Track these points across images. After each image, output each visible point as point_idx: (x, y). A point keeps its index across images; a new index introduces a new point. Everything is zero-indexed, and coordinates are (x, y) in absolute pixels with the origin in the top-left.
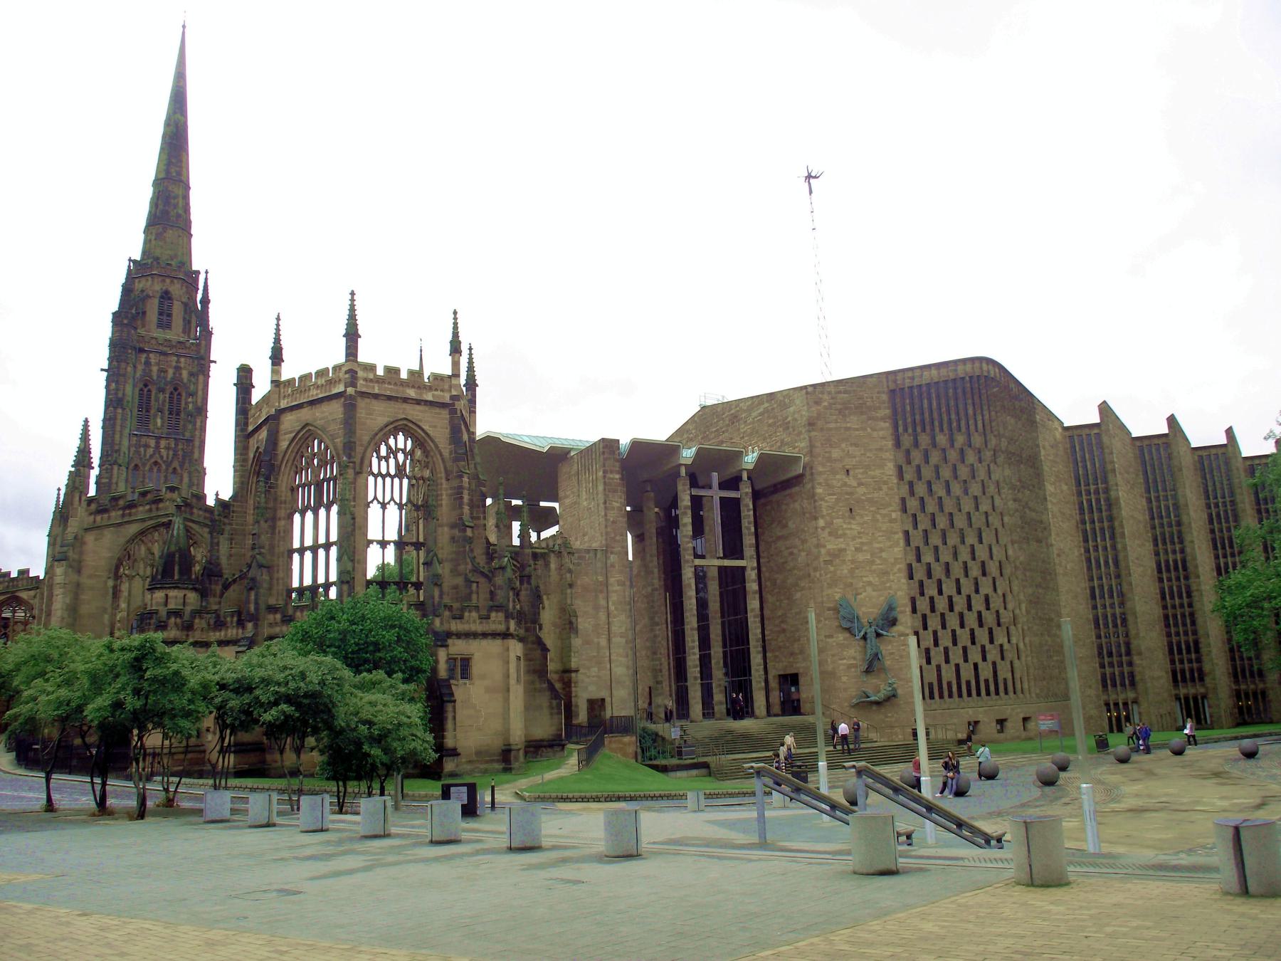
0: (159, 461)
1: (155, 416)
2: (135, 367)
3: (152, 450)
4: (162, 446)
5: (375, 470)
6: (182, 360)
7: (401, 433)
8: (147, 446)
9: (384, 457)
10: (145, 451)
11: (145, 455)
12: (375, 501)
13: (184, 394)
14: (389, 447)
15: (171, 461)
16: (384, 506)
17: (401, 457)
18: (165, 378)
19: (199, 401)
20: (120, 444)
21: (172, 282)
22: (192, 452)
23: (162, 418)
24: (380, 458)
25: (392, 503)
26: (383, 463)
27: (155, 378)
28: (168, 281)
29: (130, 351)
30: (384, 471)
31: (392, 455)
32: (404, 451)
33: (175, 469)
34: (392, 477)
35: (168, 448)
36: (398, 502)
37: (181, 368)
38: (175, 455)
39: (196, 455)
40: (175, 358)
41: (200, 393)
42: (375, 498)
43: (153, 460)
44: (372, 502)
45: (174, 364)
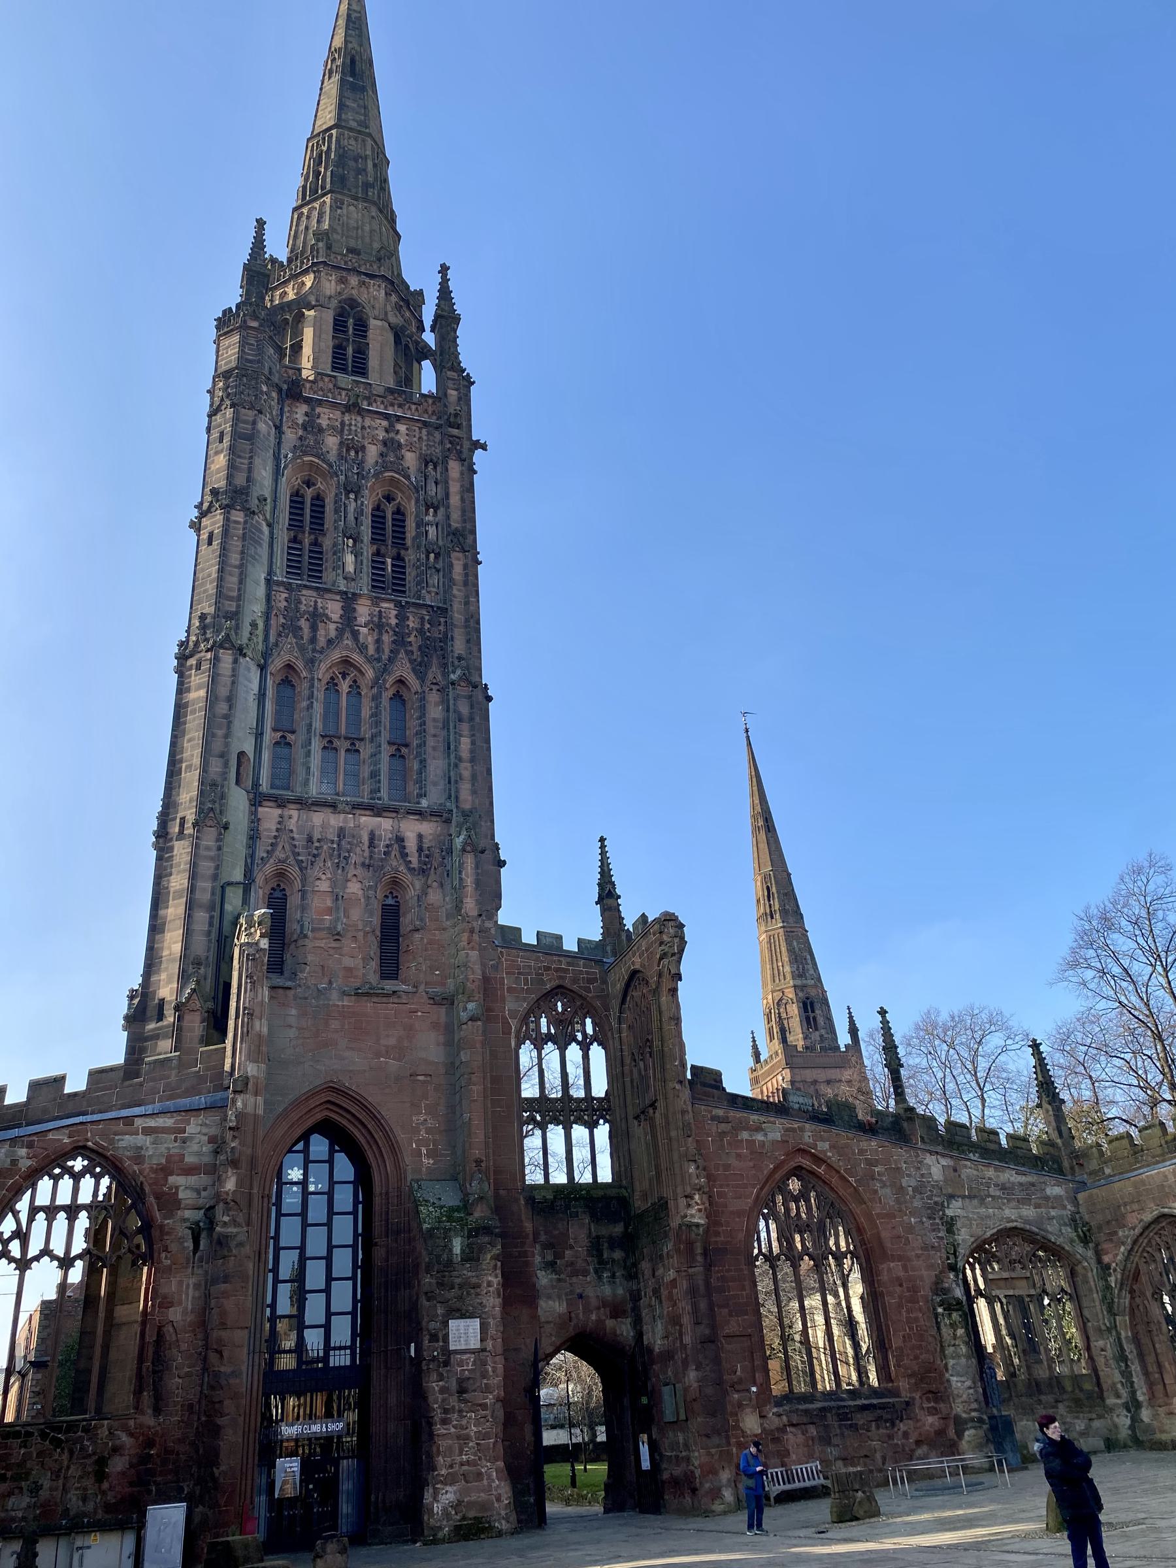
0: (356, 658)
1: (338, 552)
2: (278, 428)
3: (332, 627)
4: (362, 620)
6: (402, 428)
8: (317, 617)
10: (314, 628)
11: (313, 640)
13: (411, 508)
15: (391, 660)
18: (360, 465)
19: (455, 515)
20: (239, 598)
21: (362, 284)
22: (446, 638)
23: (357, 555)
27: (332, 457)
28: (354, 280)
29: (265, 388)
33: (401, 682)
35: (378, 625)
37: (400, 446)
38: (400, 641)
39: (459, 646)
40: (385, 423)
41: (455, 500)
43: (336, 655)
45: (382, 435)
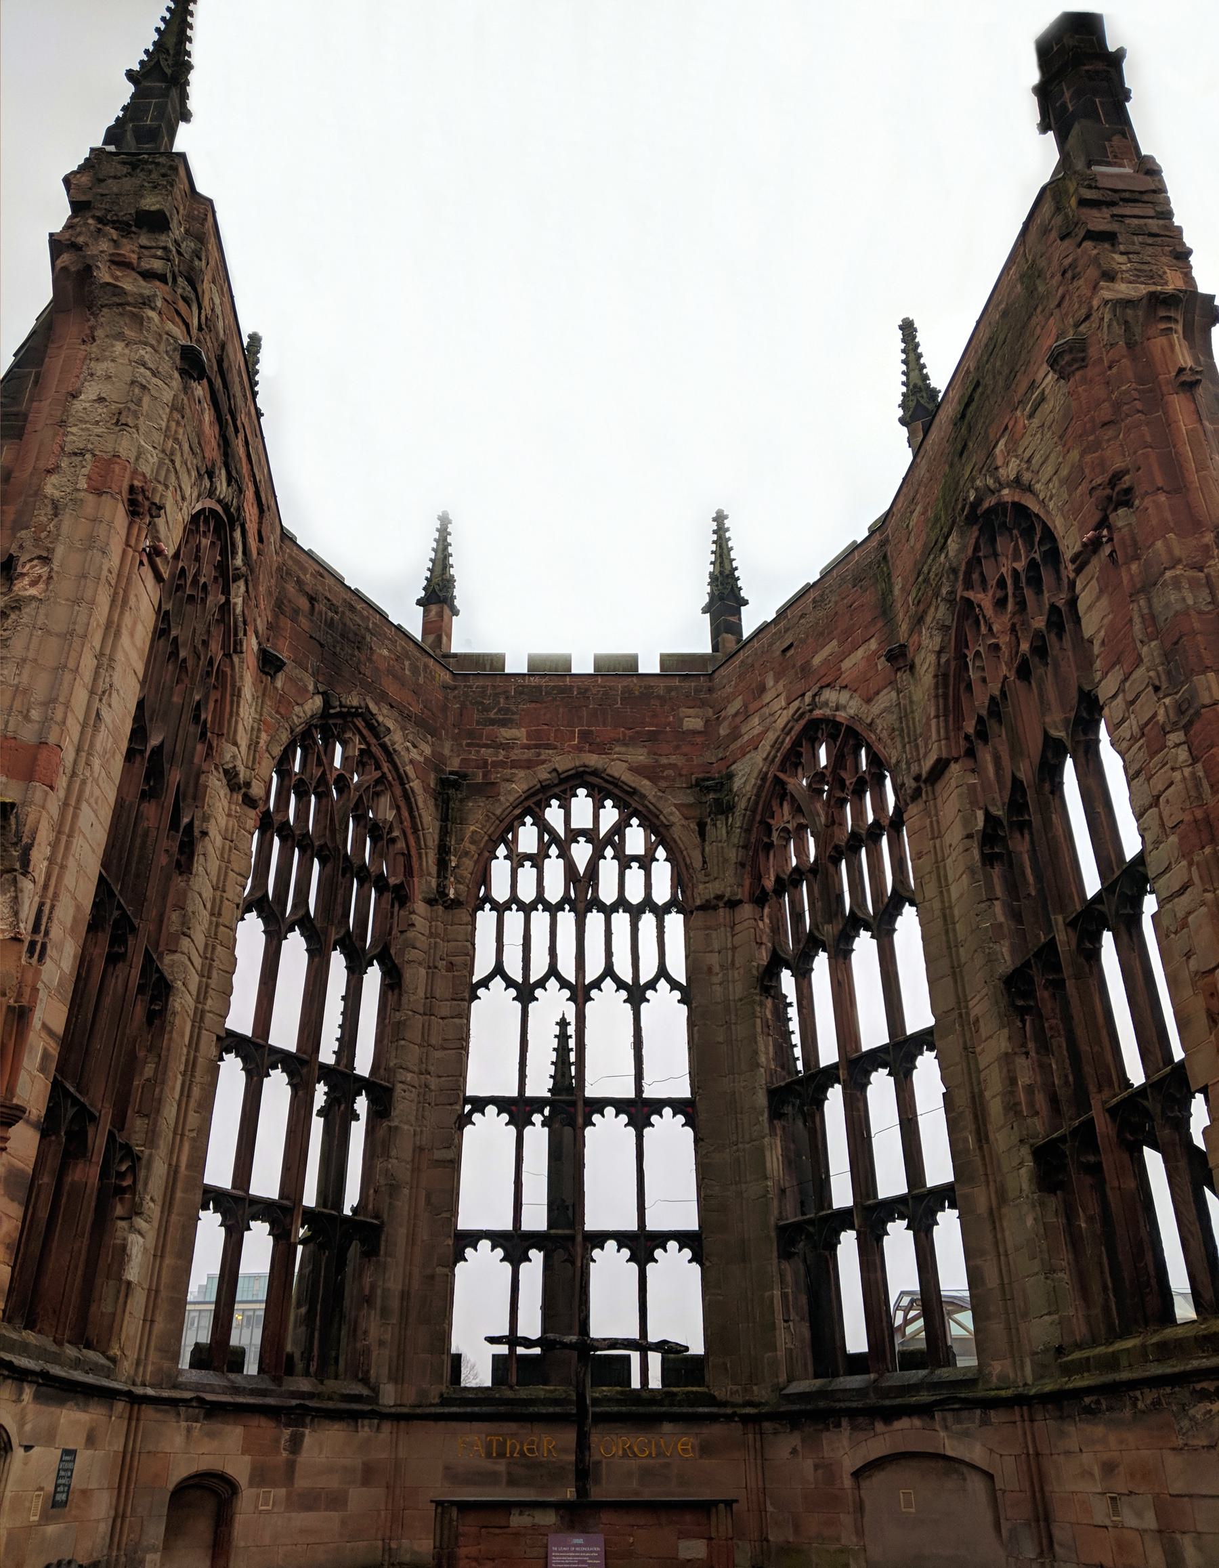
5: (501, 893)
7: (582, 792)
9: (528, 857)
12: (498, 982)
14: (543, 826)
16: (525, 993)
17: (581, 852)
24: (517, 860)
25: (552, 983)
26: (527, 874)
30: (527, 893)
31: (554, 851)
32: (590, 835)
34: (553, 910)
36: (571, 978)
42: (499, 970)
44: (485, 983)
